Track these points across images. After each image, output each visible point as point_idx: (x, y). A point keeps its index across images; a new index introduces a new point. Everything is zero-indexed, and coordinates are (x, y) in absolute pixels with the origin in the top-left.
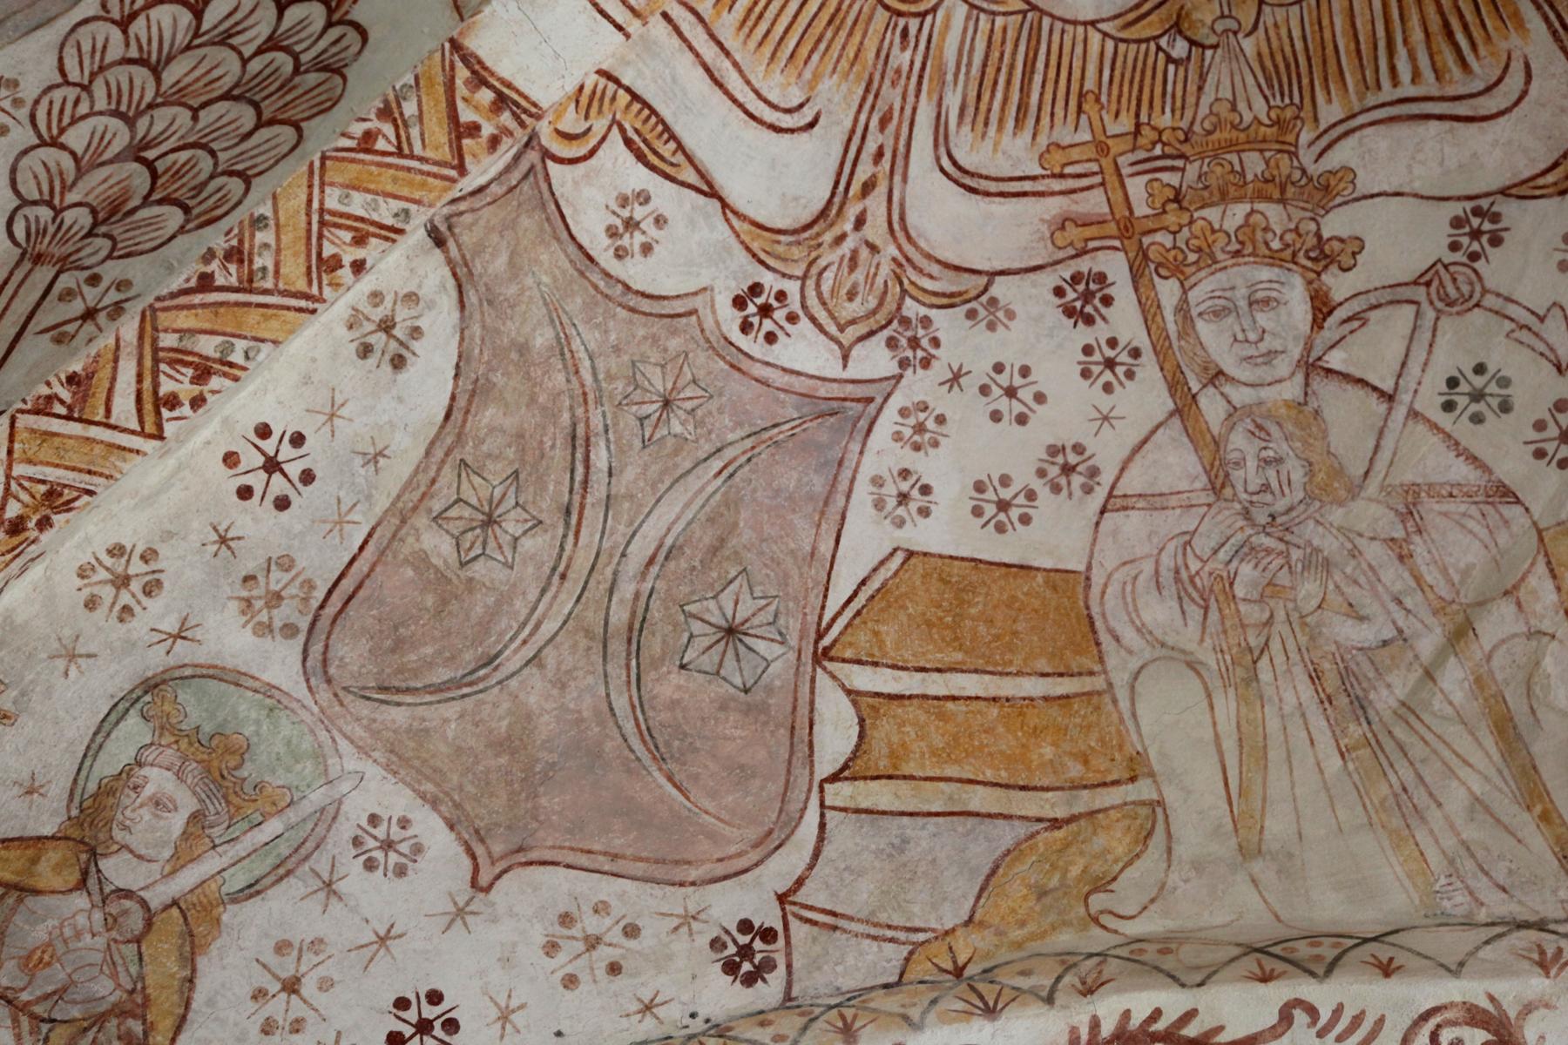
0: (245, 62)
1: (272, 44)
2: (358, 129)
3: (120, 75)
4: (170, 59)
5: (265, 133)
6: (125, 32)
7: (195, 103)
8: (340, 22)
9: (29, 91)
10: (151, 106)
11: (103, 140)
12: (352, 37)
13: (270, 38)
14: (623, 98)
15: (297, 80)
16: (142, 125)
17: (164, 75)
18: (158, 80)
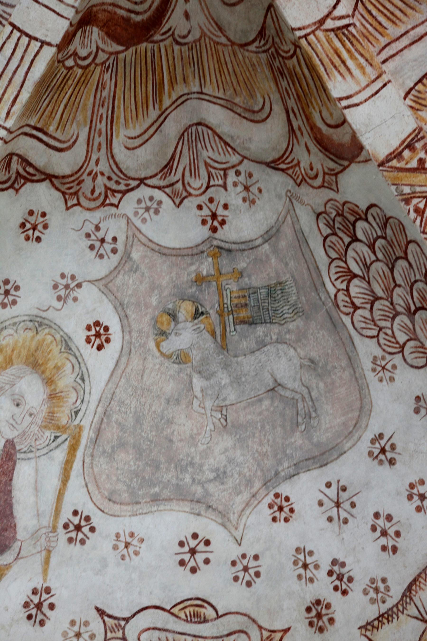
0: (378, 260)
1: (372, 246)
2: (413, 215)
3: (377, 314)
4: (372, 291)
5: (410, 257)
6: (359, 308)
7: (393, 285)
8: (366, 215)
9: (379, 353)
10: (392, 304)
11: (404, 327)
12: (372, 211)
13: (369, 247)
14: (420, 87)
15: (388, 238)
16: (399, 309)
17: (379, 295)
18: (381, 298)
